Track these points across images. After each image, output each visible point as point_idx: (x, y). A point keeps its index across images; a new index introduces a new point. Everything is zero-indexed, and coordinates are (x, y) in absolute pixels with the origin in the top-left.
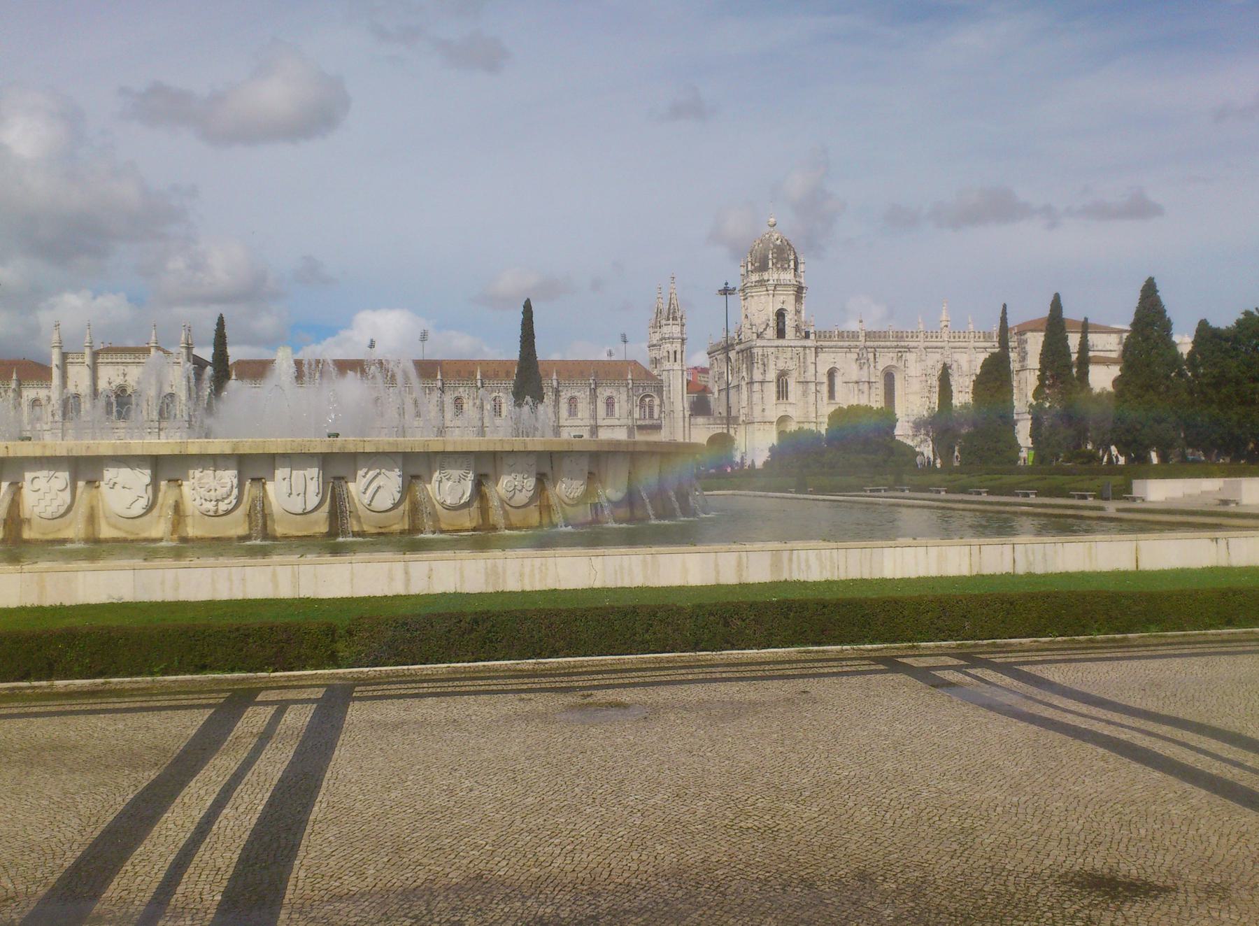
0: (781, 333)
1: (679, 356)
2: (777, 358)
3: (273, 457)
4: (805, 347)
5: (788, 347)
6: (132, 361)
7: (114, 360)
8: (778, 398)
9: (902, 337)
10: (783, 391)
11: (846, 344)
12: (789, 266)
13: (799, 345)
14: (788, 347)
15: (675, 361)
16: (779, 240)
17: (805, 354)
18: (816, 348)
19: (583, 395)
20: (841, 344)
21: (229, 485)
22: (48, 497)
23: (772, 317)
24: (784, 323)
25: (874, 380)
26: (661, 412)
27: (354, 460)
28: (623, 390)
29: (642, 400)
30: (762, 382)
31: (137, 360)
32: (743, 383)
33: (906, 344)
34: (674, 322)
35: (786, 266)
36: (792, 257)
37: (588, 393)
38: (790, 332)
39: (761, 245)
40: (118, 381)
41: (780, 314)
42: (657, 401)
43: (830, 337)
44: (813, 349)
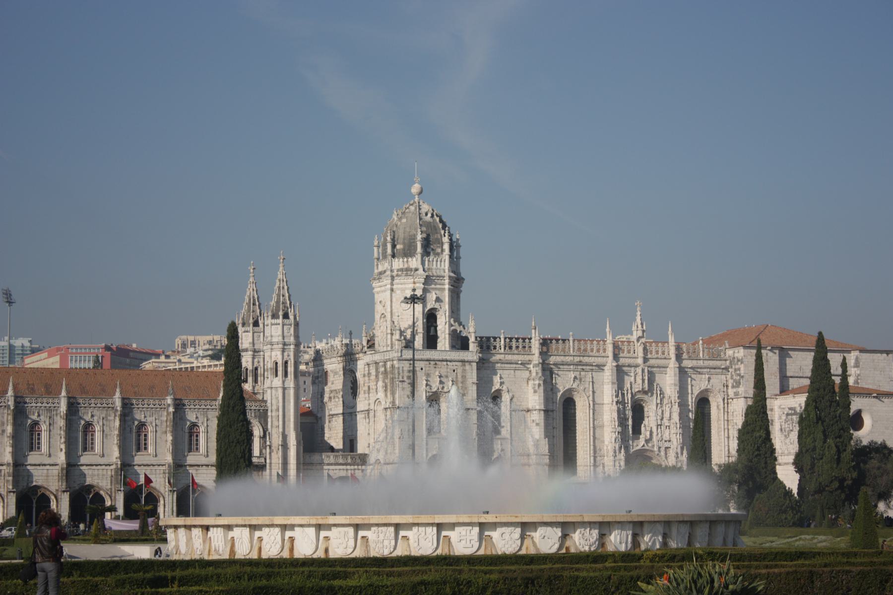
1: (291, 369)
2: (428, 375)
3: (574, 523)
4: (463, 361)
5: (443, 361)
9: (585, 350)
12: (443, 250)
13: (457, 358)
14: (443, 361)
15: (286, 374)
16: (429, 215)
17: (464, 370)
20: (509, 357)
21: (595, 538)
22: (510, 543)
24: (436, 327)
25: (550, 407)
26: (263, 446)
27: (534, 526)
32: (380, 409)
33: (591, 360)
34: (286, 321)
35: (439, 250)
36: (446, 239)
37: (165, 419)
38: (444, 341)
39: (404, 220)
41: (431, 318)
44: (474, 365)
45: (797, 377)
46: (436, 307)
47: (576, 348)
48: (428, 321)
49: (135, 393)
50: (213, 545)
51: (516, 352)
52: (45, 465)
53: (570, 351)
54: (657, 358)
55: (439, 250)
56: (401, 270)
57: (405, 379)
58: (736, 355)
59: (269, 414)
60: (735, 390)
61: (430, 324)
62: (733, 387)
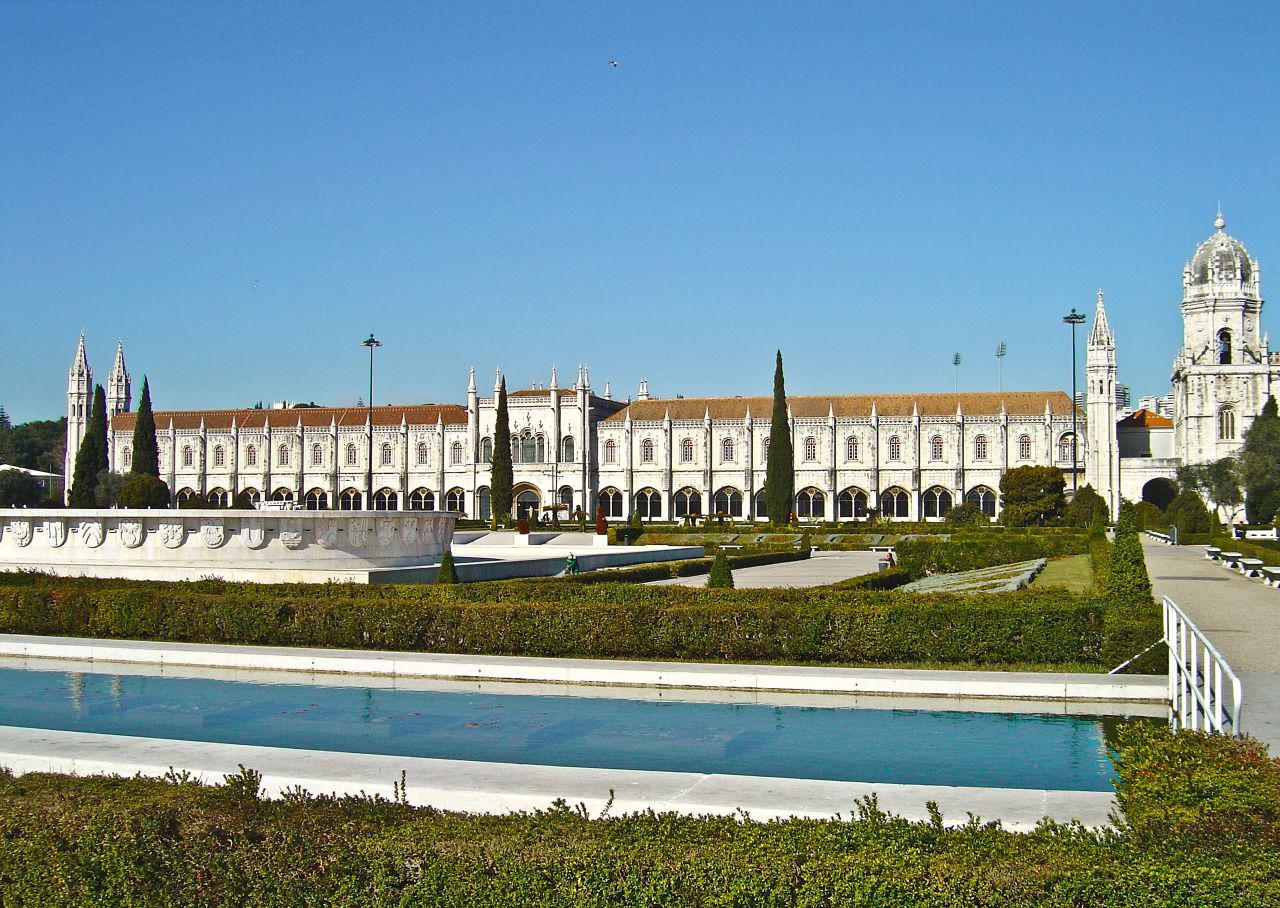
0: (1226, 358)
2: (1218, 388)
6: (536, 404)
7: (520, 405)
8: (1222, 436)
10: (1227, 428)
12: (1235, 276)
15: (1101, 393)
18: (1270, 374)
19: (992, 432)
28: (1040, 427)
29: (1062, 438)
30: (1198, 417)
31: (539, 404)
34: (1102, 347)
40: (523, 424)
41: (1224, 335)
42: (1080, 439)
44: (1266, 376)
55: (1231, 276)
56: (1197, 296)
57: (1195, 391)
59: (1089, 425)
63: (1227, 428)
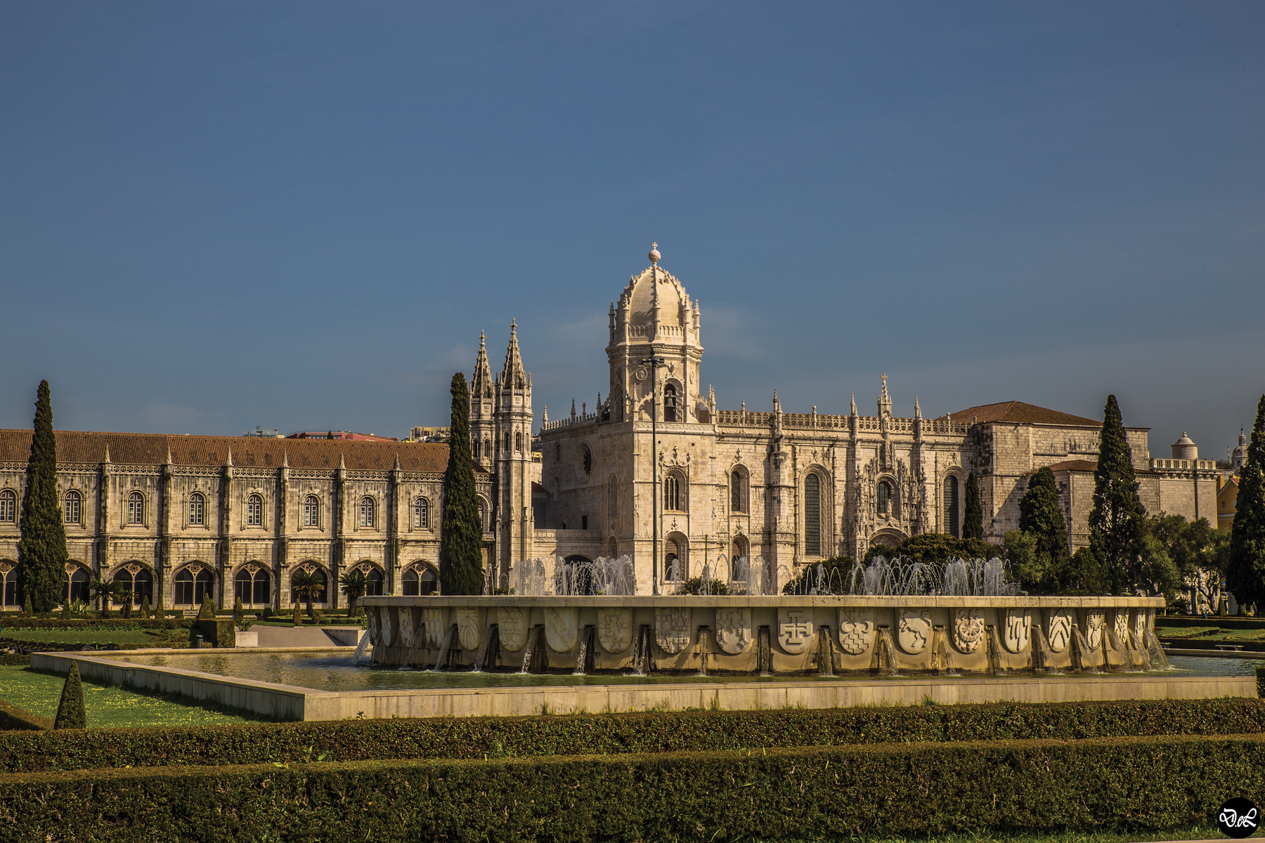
4: (702, 434)
8: (667, 508)
9: (830, 425)
10: (672, 497)
11: (756, 432)
23: (660, 389)
24: (674, 399)
34: (520, 391)
43: (735, 421)
45: (1048, 455)
46: (675, 377)
47: (820, 422)
48: (666, 393)
49: (360, 465)
50: (428, 635)
51: (757, 426)
52: (264, 539)
53: (813, 425)
54: (903, 434)
58: (985, 432)
60: (983, 468)
61: (667, 396)
62: (981, 465)
63: (672, 497)
